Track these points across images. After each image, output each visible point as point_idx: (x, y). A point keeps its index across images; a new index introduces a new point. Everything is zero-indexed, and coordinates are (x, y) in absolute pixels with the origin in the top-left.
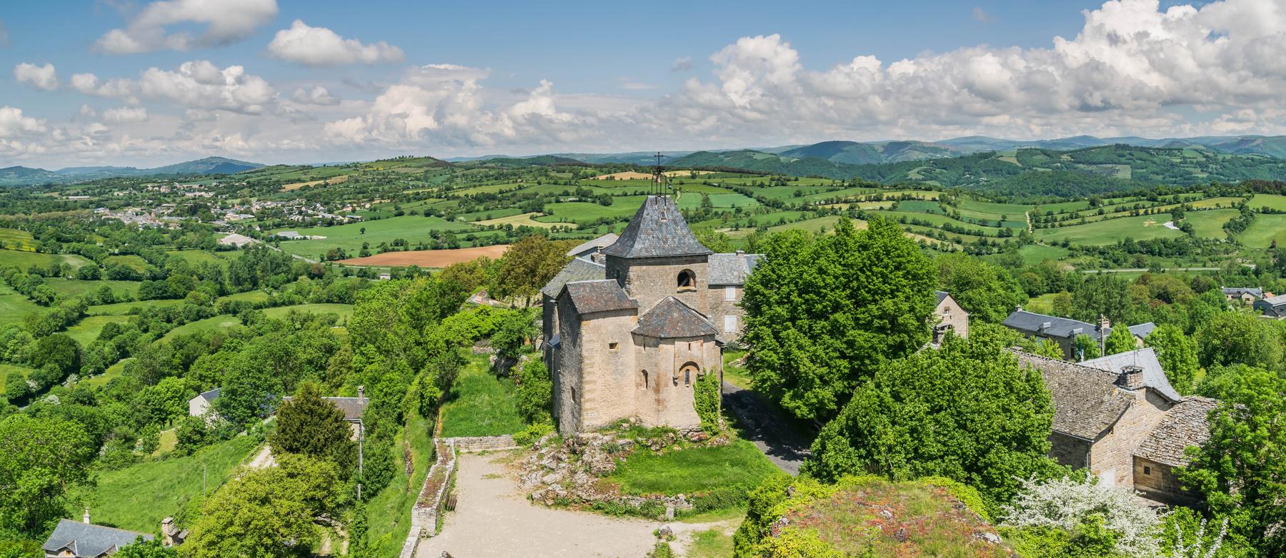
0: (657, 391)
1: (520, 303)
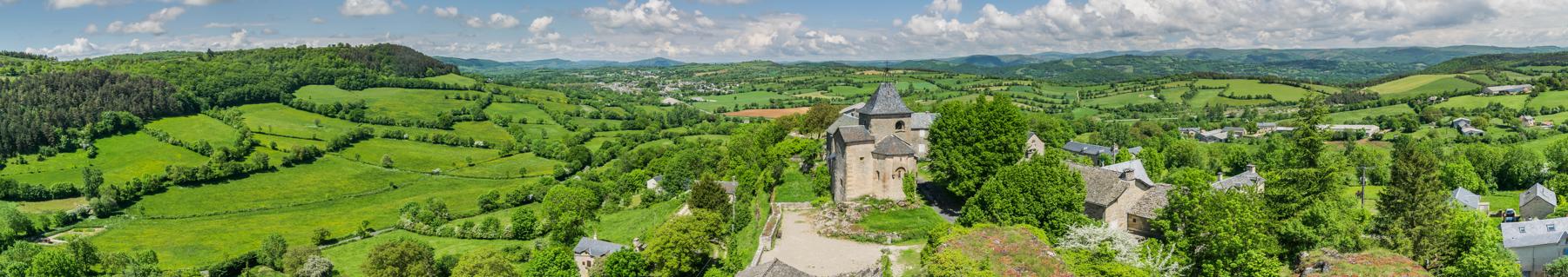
1: (815, 136)
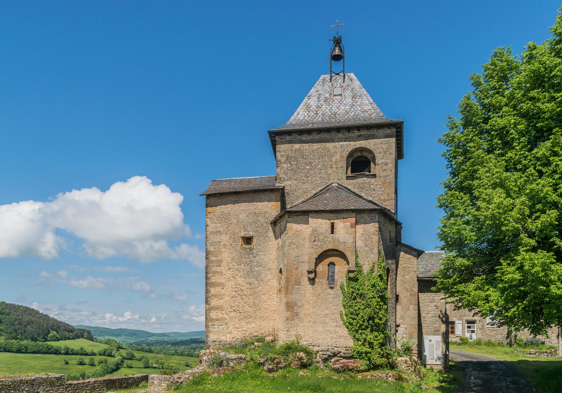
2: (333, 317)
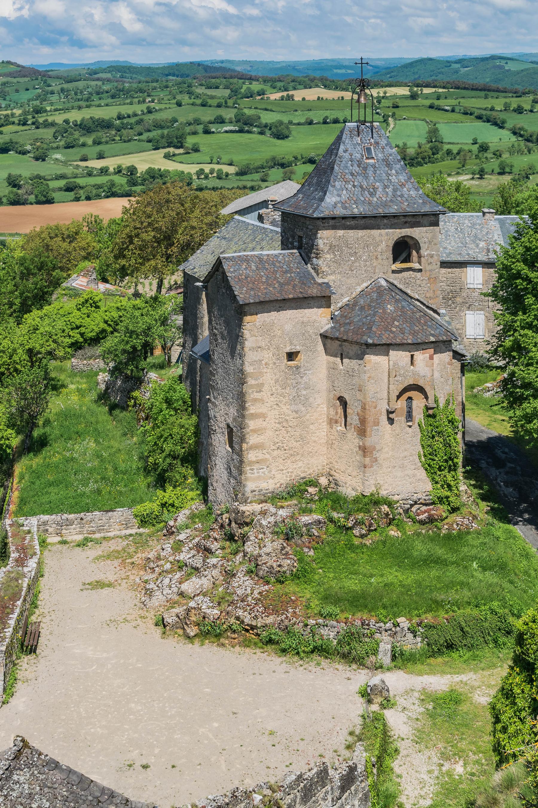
0: (362, 432)
1: (148, 287)
2: (411, 458)
